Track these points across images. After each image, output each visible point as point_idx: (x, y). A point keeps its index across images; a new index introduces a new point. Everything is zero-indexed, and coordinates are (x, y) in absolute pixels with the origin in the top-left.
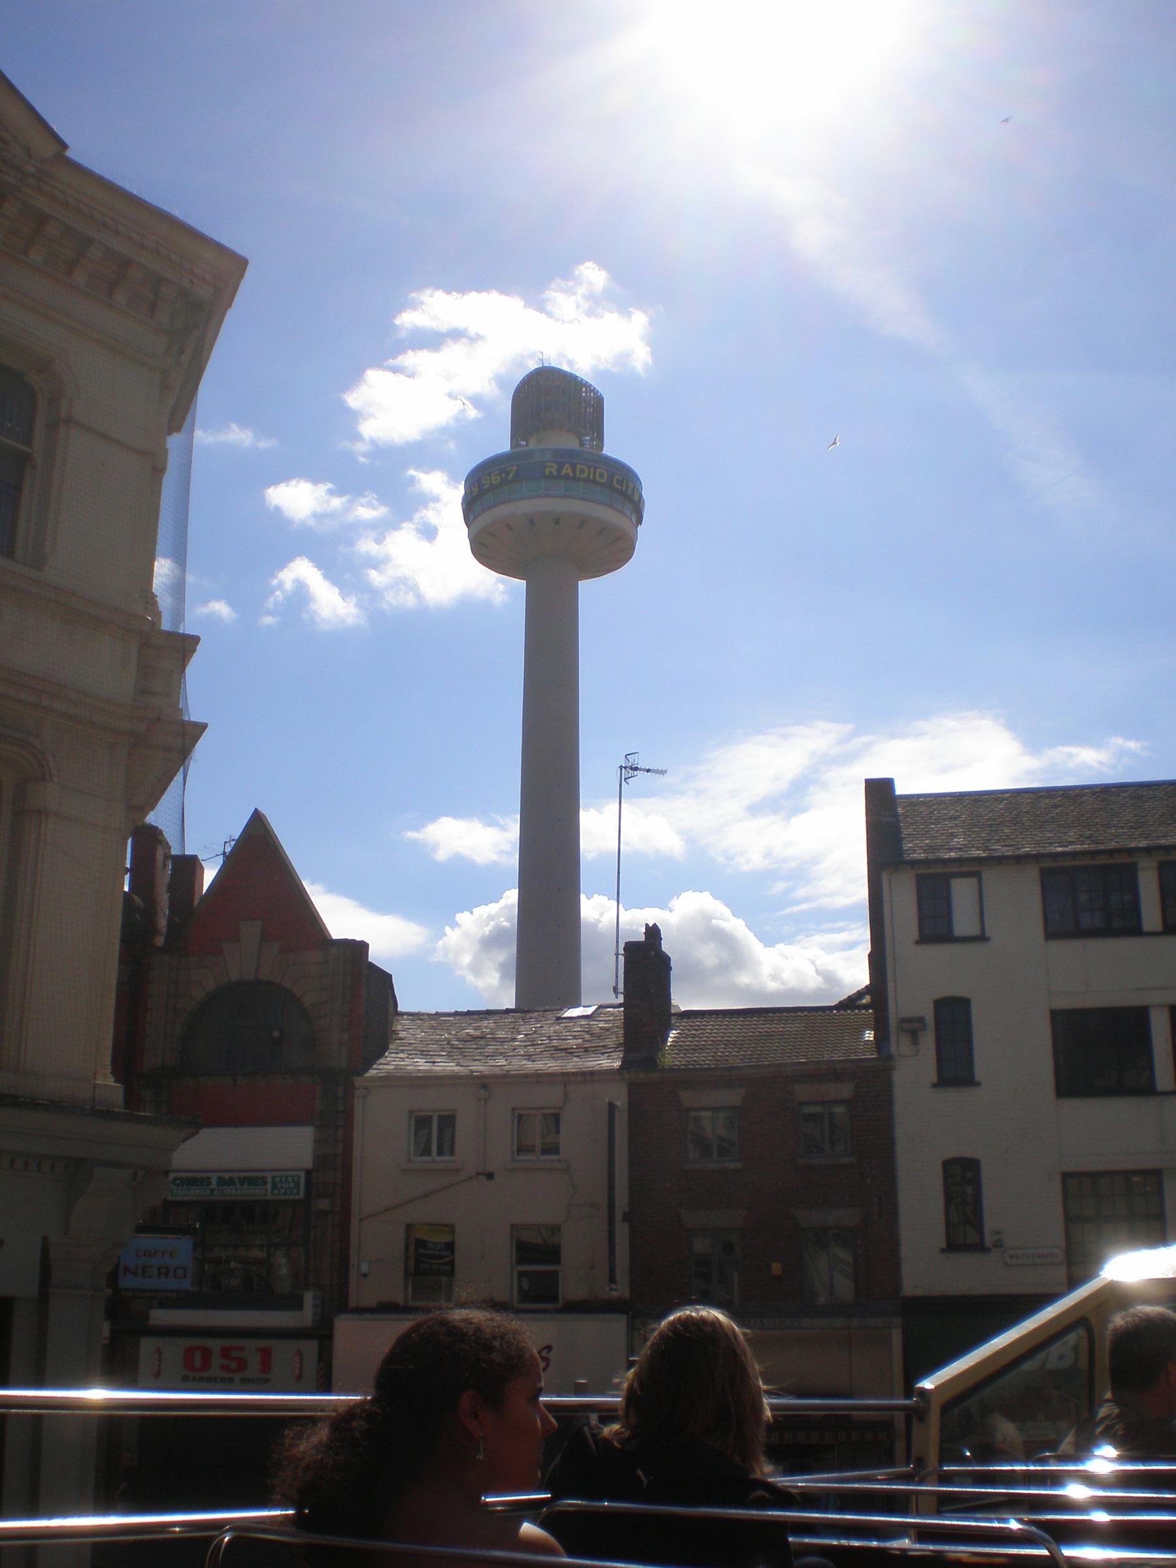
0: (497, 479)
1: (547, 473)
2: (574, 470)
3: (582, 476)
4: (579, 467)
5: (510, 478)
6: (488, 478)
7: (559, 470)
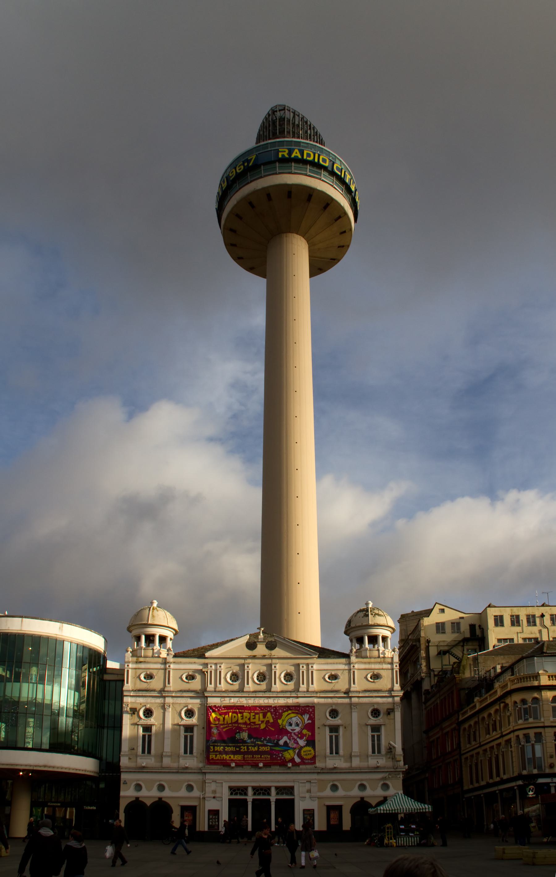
0: (239, 170)
1: (280, 156)
2: (302, 155)
3: (308, 159)
4: (305, 152)
5: (251, 164)
6: (234, 170)
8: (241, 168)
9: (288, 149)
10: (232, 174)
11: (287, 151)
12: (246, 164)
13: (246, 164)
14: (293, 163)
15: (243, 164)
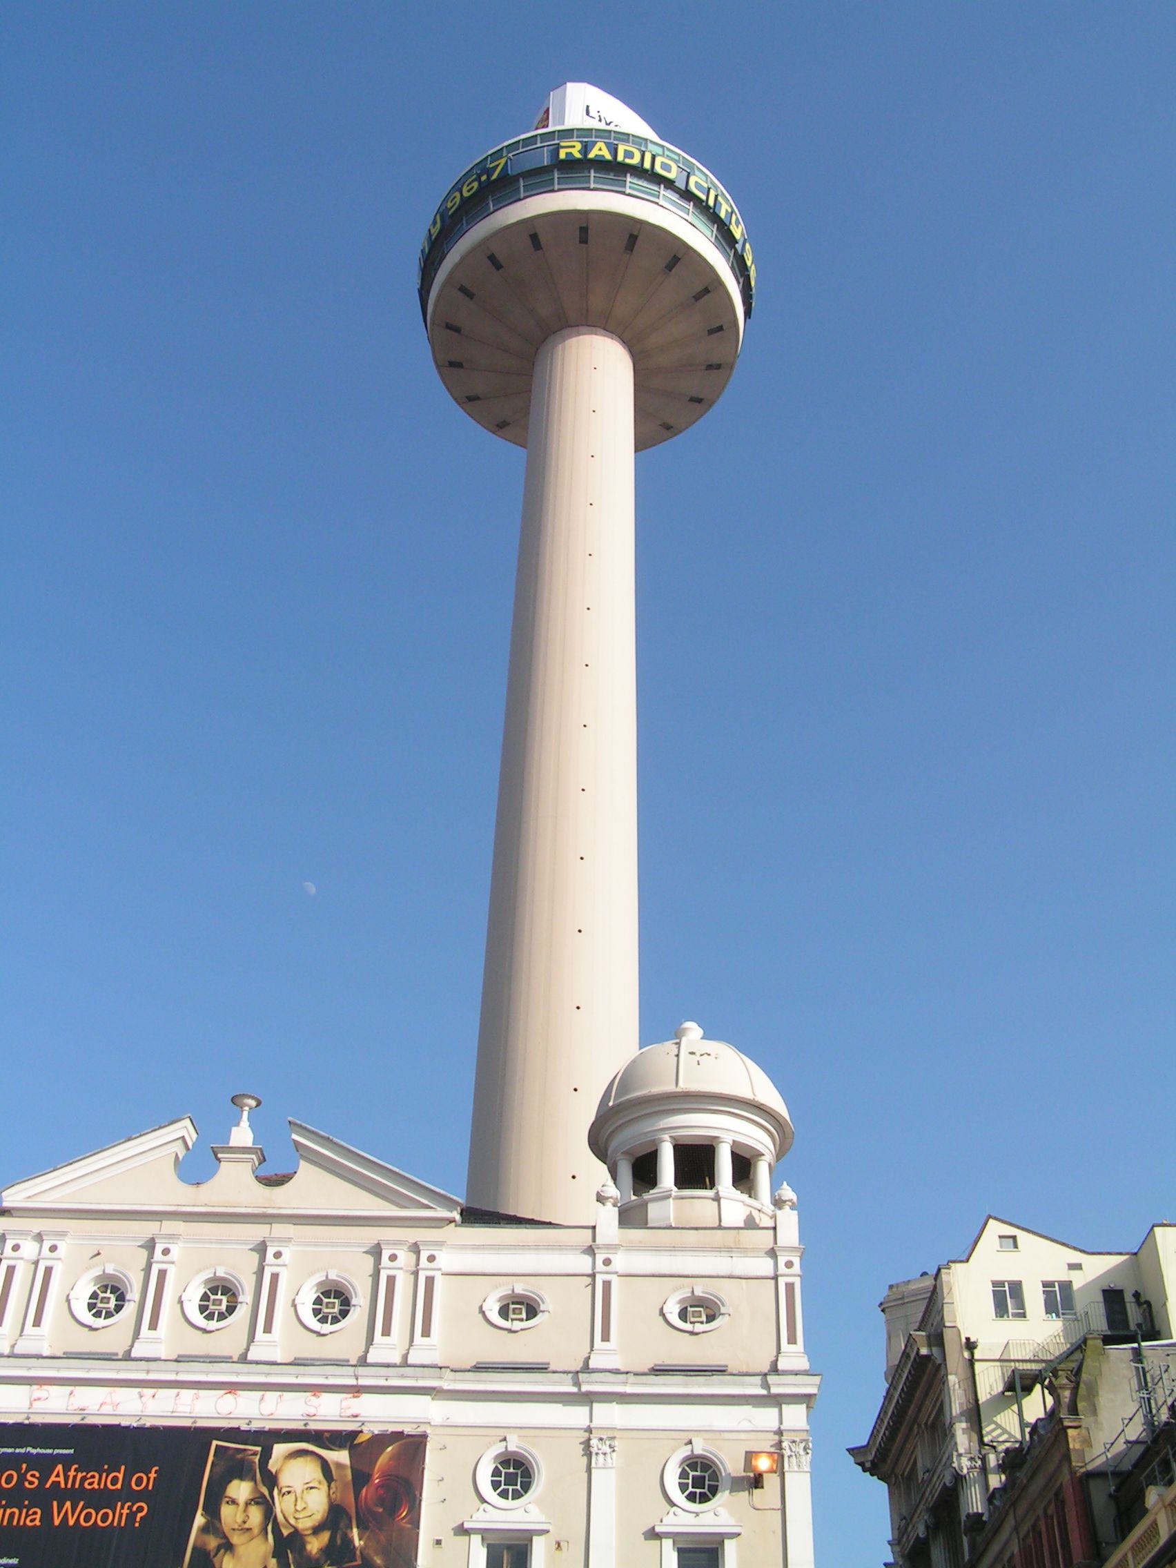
2: (614, 152)
3: (628, 161)
7: (586, 148)
8: (473, 187)
9: (581, 142)
10: (453, 202)
11: (579, 146)
12: (484, 178)
13: (484, 178)
14: (592, 171)
15: (478, 178)
